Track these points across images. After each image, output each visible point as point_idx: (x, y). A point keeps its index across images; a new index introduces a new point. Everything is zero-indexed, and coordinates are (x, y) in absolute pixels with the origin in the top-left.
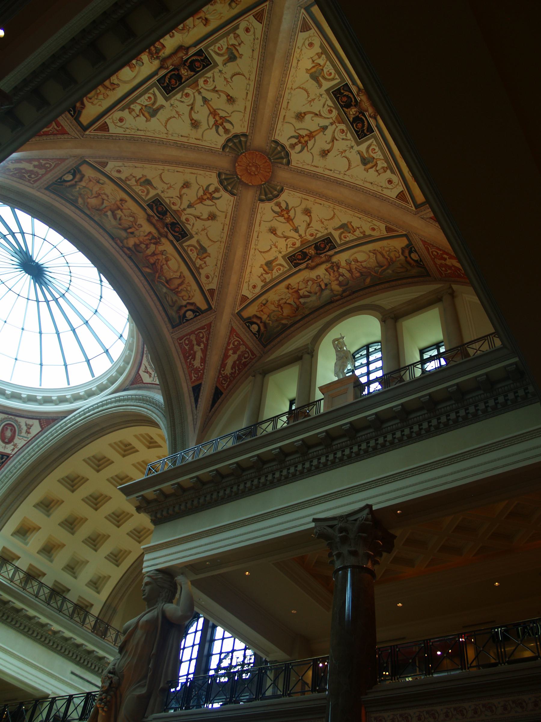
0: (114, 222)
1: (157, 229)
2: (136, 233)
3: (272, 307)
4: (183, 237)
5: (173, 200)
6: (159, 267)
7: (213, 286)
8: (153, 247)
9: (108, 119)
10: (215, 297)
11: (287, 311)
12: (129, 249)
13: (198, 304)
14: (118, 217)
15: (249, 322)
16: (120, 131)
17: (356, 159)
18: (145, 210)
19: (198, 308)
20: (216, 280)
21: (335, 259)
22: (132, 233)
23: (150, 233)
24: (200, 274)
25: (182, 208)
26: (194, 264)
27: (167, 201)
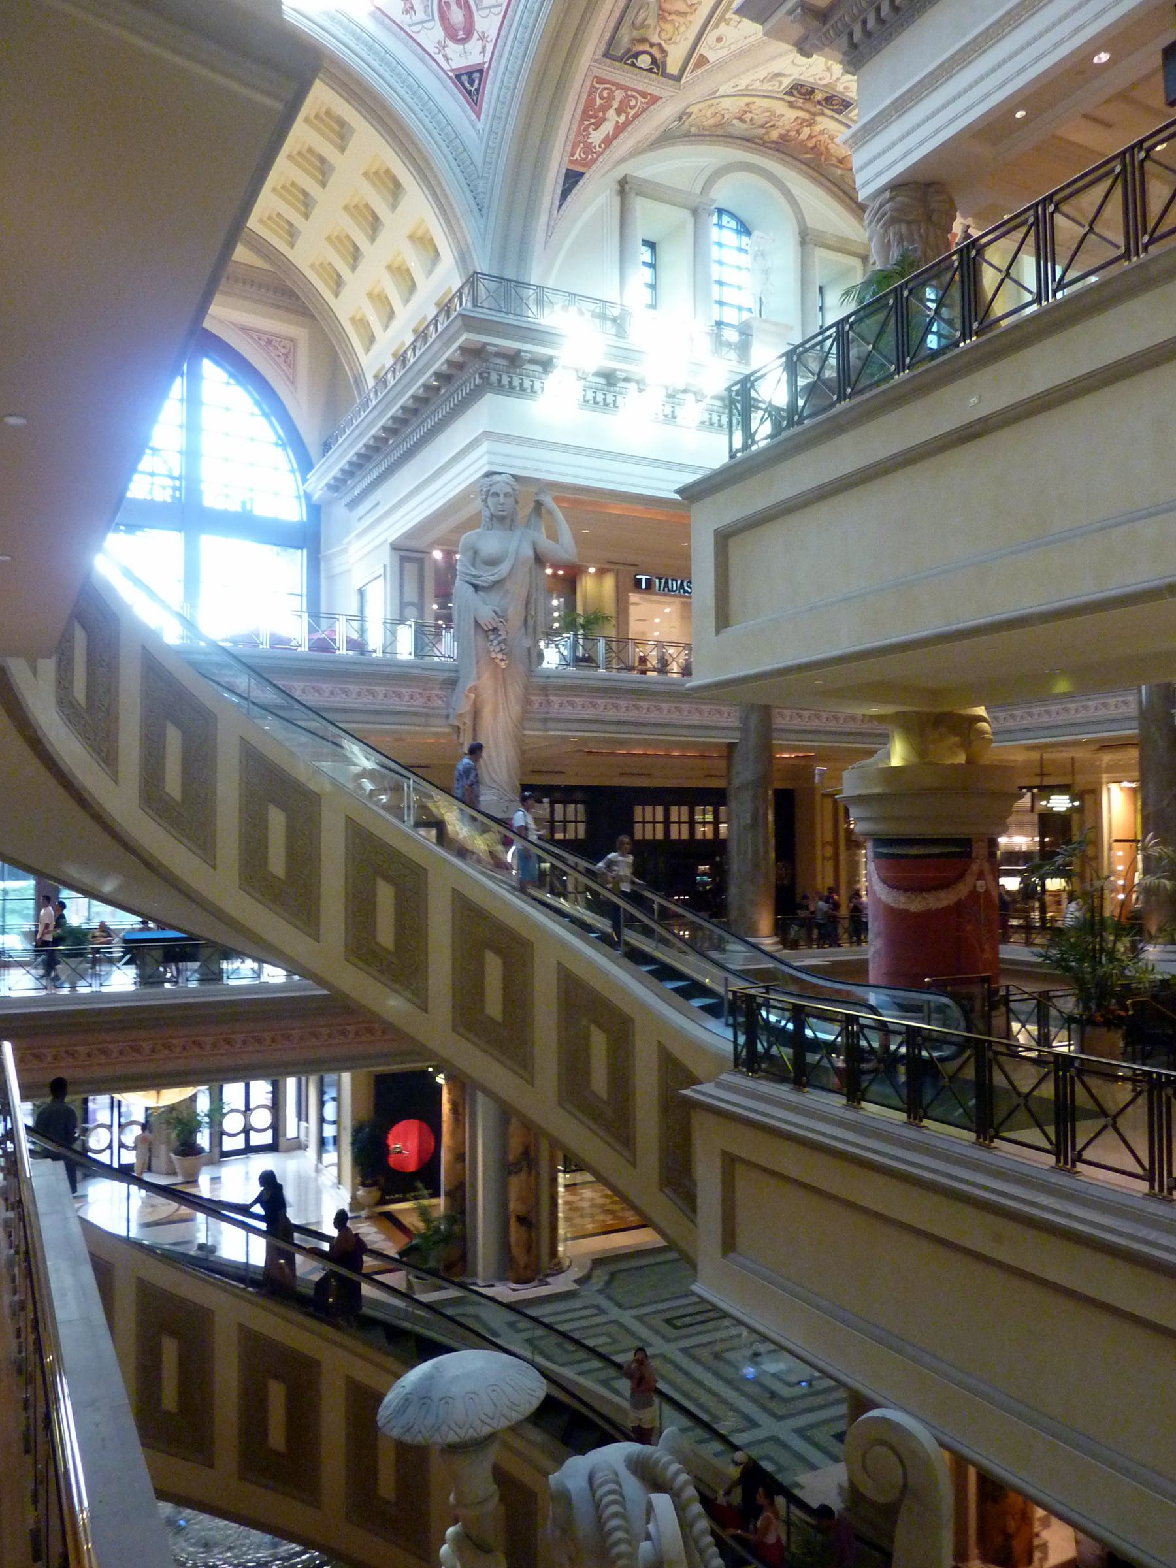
0: (744, 126)
1: (808, 111)
2: (779, 124)
4: (847, 107)
5: (817, 77)
6: (823, 149)
8: (806, 131)
9: (702, 50)
12: (773, 142)
14: (748, 120)
16: (725, 52)
18: (783, 99)
22: (773, 126)
23: (797, 118)
25: (834, 78)
27: (811, 80)
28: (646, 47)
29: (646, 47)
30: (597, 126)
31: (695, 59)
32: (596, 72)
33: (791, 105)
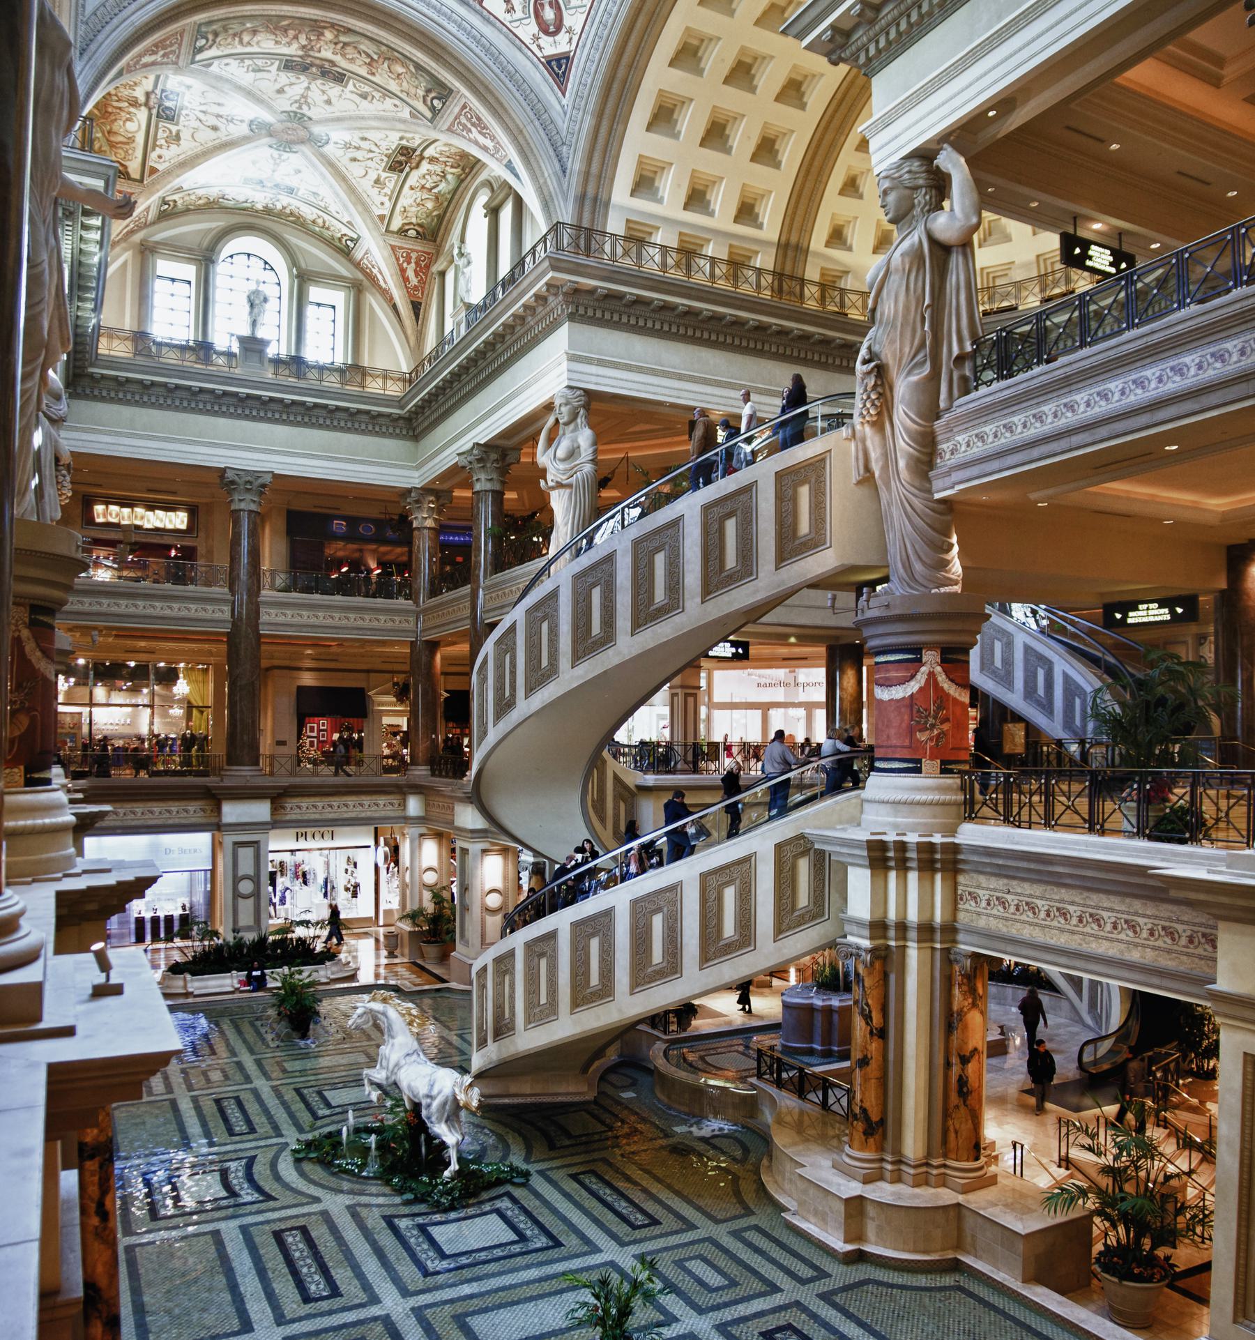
3: (193, 197)
7: (160, 167)
9: (216, 62)
10: (155, 176)
11: (201, 202)
13: (130, 170)
15: (165, 203)
17: (373, 176)
19: (128, 173)
20: (167, 164)
21: (280, 197)
24: (154, 149)
26: (155, 139)
28: (210, 37)
29: (210, 37)
30: (154, 53)
31: (208, 63)
32: (187, 28)
33: (148, 95)
